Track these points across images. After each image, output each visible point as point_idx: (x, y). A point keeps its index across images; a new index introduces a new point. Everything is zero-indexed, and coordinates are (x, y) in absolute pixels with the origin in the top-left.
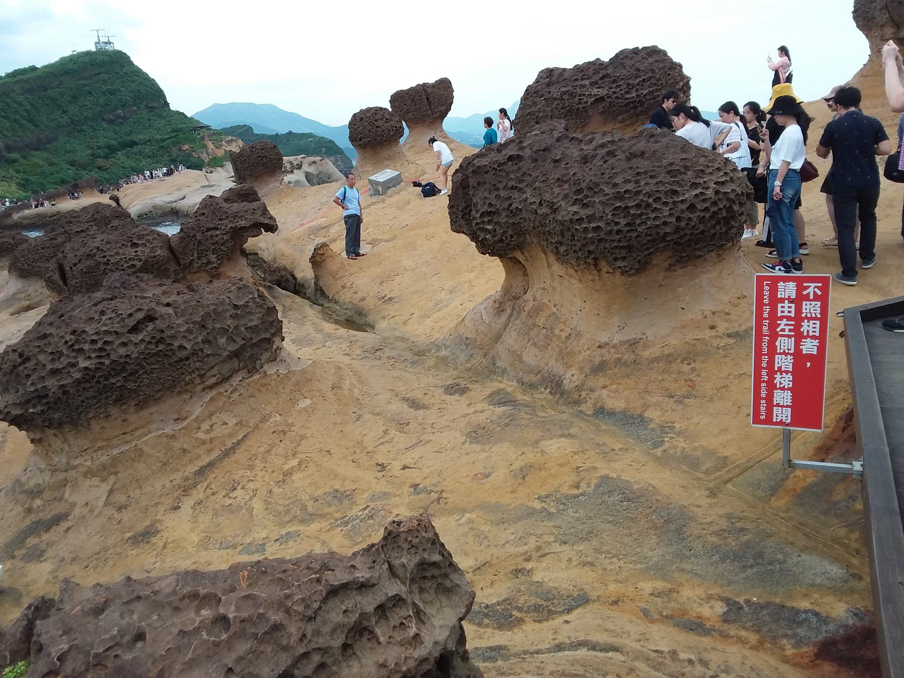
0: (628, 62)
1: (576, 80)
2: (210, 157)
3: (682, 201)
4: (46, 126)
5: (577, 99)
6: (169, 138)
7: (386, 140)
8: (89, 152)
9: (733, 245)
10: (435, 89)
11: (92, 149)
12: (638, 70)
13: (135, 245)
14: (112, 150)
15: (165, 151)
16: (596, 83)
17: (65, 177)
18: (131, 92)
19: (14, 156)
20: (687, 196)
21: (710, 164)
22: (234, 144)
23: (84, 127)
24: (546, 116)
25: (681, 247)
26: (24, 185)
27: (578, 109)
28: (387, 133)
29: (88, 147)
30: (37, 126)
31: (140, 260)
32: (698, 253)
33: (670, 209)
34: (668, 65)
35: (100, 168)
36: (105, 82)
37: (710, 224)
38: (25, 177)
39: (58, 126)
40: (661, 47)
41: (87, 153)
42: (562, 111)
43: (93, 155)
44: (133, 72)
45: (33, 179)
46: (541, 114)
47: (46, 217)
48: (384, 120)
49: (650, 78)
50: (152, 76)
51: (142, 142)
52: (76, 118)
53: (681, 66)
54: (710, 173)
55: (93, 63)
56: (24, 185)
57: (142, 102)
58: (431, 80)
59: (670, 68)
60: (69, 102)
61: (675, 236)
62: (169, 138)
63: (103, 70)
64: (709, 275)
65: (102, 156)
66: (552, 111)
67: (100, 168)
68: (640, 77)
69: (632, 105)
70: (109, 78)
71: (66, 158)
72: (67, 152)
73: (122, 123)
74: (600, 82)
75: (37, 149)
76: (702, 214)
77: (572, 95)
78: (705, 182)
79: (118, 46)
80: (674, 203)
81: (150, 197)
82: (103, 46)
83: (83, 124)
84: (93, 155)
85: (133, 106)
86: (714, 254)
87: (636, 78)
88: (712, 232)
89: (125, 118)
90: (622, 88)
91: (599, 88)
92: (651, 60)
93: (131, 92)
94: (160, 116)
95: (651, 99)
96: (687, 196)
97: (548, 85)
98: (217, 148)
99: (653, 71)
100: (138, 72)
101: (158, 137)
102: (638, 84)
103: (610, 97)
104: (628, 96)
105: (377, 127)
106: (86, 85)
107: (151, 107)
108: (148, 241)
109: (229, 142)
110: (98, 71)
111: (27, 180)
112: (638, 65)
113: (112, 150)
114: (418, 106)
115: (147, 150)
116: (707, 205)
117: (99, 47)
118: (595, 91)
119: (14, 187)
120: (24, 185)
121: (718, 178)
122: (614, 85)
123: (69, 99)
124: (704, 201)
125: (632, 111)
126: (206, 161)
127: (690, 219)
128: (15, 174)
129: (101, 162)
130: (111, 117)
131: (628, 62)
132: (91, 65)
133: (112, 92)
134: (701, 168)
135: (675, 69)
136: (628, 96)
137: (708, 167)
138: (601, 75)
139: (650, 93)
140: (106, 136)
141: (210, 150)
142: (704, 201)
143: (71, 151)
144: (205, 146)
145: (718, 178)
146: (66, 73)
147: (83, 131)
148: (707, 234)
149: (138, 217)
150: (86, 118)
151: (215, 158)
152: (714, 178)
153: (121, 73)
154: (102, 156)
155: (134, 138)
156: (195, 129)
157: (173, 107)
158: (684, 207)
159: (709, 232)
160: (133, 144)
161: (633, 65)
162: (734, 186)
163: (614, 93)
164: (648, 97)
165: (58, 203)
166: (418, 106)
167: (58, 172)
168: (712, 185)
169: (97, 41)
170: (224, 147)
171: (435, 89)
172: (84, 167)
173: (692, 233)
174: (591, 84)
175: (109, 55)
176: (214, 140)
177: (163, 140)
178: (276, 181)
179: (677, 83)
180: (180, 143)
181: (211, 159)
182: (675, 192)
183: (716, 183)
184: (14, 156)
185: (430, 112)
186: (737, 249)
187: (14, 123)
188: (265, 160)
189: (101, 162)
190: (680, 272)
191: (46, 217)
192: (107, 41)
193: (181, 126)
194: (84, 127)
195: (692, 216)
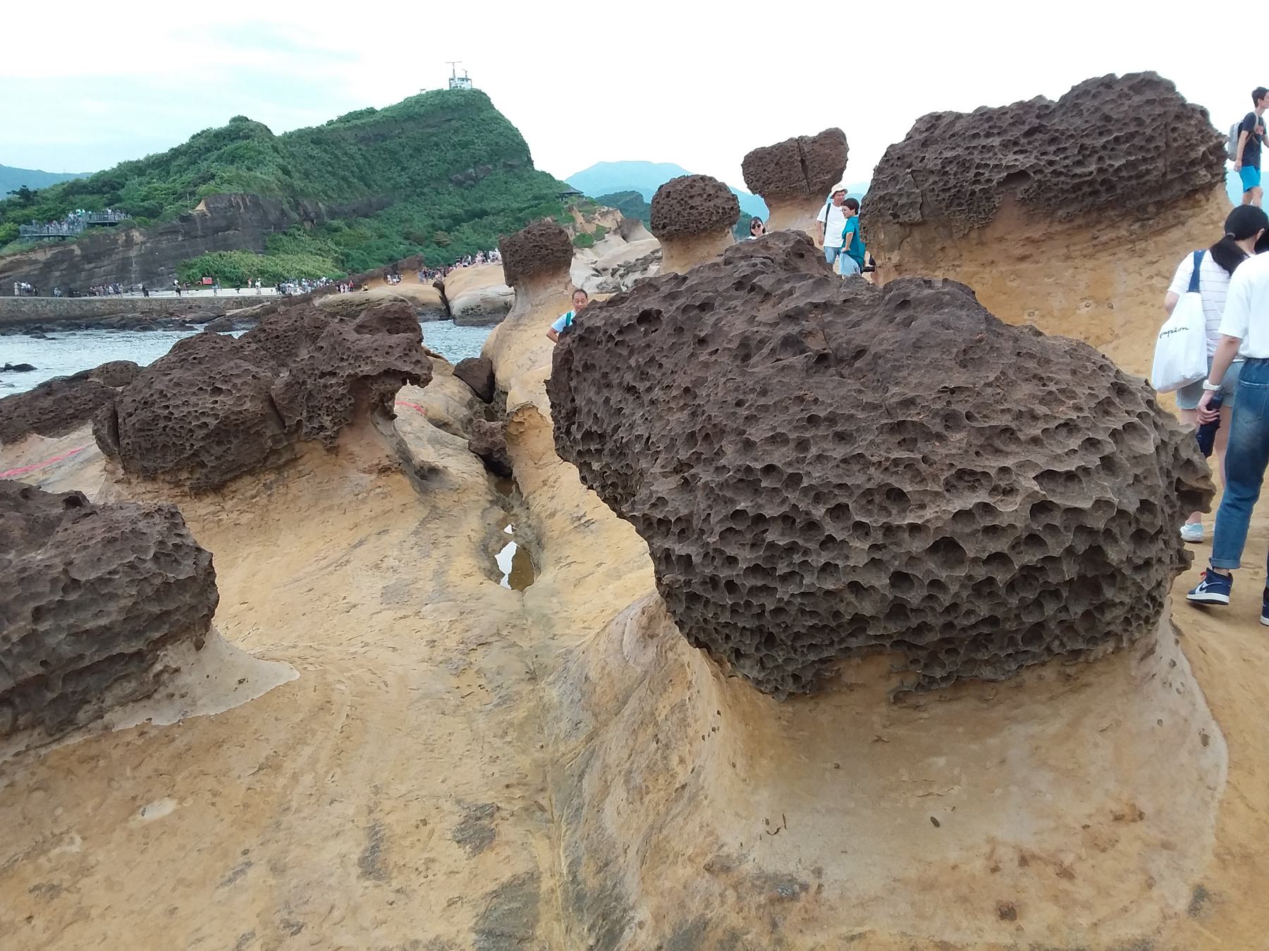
0: (1088, 103)
1: (976, 136)
3: (914, 529)
4: (380, 187)
5: (971, 174)
6: (529, 208)
7: (705, 229)
8: (428, 222)
9: (1118, 649)
10: (816, 146)
12: (1108, 119)
13: (217, 391)
14: (457, 220)
15: (522, 224)
16: (1016, 143)
17: (395, 254)
18: (488, 145)
19: (336, 223)
20: (929, 514)
21: (1041, 410)
22: (610, 217)
23: (425, 190)
24: (912, 204)
25: (923, 654)
26: (342, 262)
27: (973, 193)
28: (707, 218)
29: (428, 215)
30: (369, 186)
31: (216, 416)
32: (987, 673)
33: (874, 547)
34: (1174, 110)
35: (438, 244)
36: (456, 131)
37: (1014, 601)
38: (346, 251)
39: (396, 187)
40: (1164, 74)
41: (426, 223)
42: (942, 196)
43: (433, 226)
44: (491, 119)
45: (354, 253)
46: (904, 200)
47: (352, 305)
48: (705, 196)
49: (1132, 136)
50: (515, 124)
51: (493, 211)
52: (419, 178)
53: (1204, 113)
54: (1035, 441)
56: (343, 261)
57: (499, 159)
58: (812, 130)
59: (1178, 117)
60: (411, 156)
61: (893, 628)
62: (529, 208)
63: (456, 115)
64: (1035, 729)
65: (444, 228)
66: (923, 195)
67: (438, 244)
68: (1109, 132)
69: (1086, 189)
70: (462, 126)
71: (400, 229)
72: (401, 221)
73: (472, 186)
74: (1023, 141)
75: (366, 216)
76: (981, 573)
77: (964, 165)
78: (1004, 470)
79: (477, 84)
80: (888, 529)
81: (481, 286)
82: (459, 83)
83: (426, 186)
84: (433, 226)
85: (489, 163)
86: (1049, 673)
87: (1101, 134)
88: (1030, 619)
89: (476, 180)
90: (1068, 153)
91: (1022, 152)
92: (1137, 99)
93: (488, 145)
94: (520, 178)
95: (1130, 178)
96: (929, 514)
97: (925, 144)
98: (588, 222)
99: (1139, 121)
100: (499, 119)
101: (515, 205)
102: (1104, 147)
103: (1041, 171)
104: (1078, 171)
105: (692, 208)
106: (432, 135)
107: (510, 165)
108: (235, 385)
109: (604, 215)
111: (347, 256)
112: (1106, 109)
113: (457, 220)
114: (785, 173)
115: (500, 222)
116: (1001, 545)
117: (453, 85)
118: (1010, 159)
119: (329, 263)
120: (343, 261)
121: (1057, 458)
122: (1052, 148)
123: (411, 152)
124: (992, 531)
125: (1088, 201)
127: (936, 584)
128: (334, 247)
129: (441, 235)
131: (1088, 103)
132: (442, 108)
133: (464, 145)
134: (1005, 421)
135: (1190, 118)
136: (1078, 171)
137: (1034, 417)
138: (1027, 127)
139: (1131, 165)
140: (452, 202)
141: (578, 225)
142: (992, 531)
143: (407, 220)
144: (573, 219)
145: (1057, 458)
147: (423, 194)
148: (1010, 626)
149: (463, 312)
150: (431, 177)
151: (583, 236)
152: (1041, 460)
153: (478, 119)
154: (444, 228)
155: (487, 205)
156: (562, 196)
157: (538, 166)
158: (918, 545)
159: (1017, 616)
160: (482, 214)
161: (1097, 109)
162: (1106, 488)
163: (1051, 163)
164: (1124, 174)
165: (370, 288)
166: (785, 173)
167: (386, 247)
168: (1028, 483)
169: (452, 77)
170: (597, 222)
171: (816, 146)
172: (419, 241)
173: (949, 626)
174: (1005, 145)
175: (464, 96)
176: (586, 211)
177: (520, 210)
178: (559, 283)
179: (1193, 147)
180: (540, 214)
181: (578, 237)
182: (897, 496)
183: (1047, 476)
184: (336, 223)
185: (804, 183)
186: (1138, 655)
187: (342, 183)
188: (544, 252)
189: (441, 235)
190: (939, 710)
191: (352, 305)
193: (545, 192)
194: (425, 190)
195: (943, 575)
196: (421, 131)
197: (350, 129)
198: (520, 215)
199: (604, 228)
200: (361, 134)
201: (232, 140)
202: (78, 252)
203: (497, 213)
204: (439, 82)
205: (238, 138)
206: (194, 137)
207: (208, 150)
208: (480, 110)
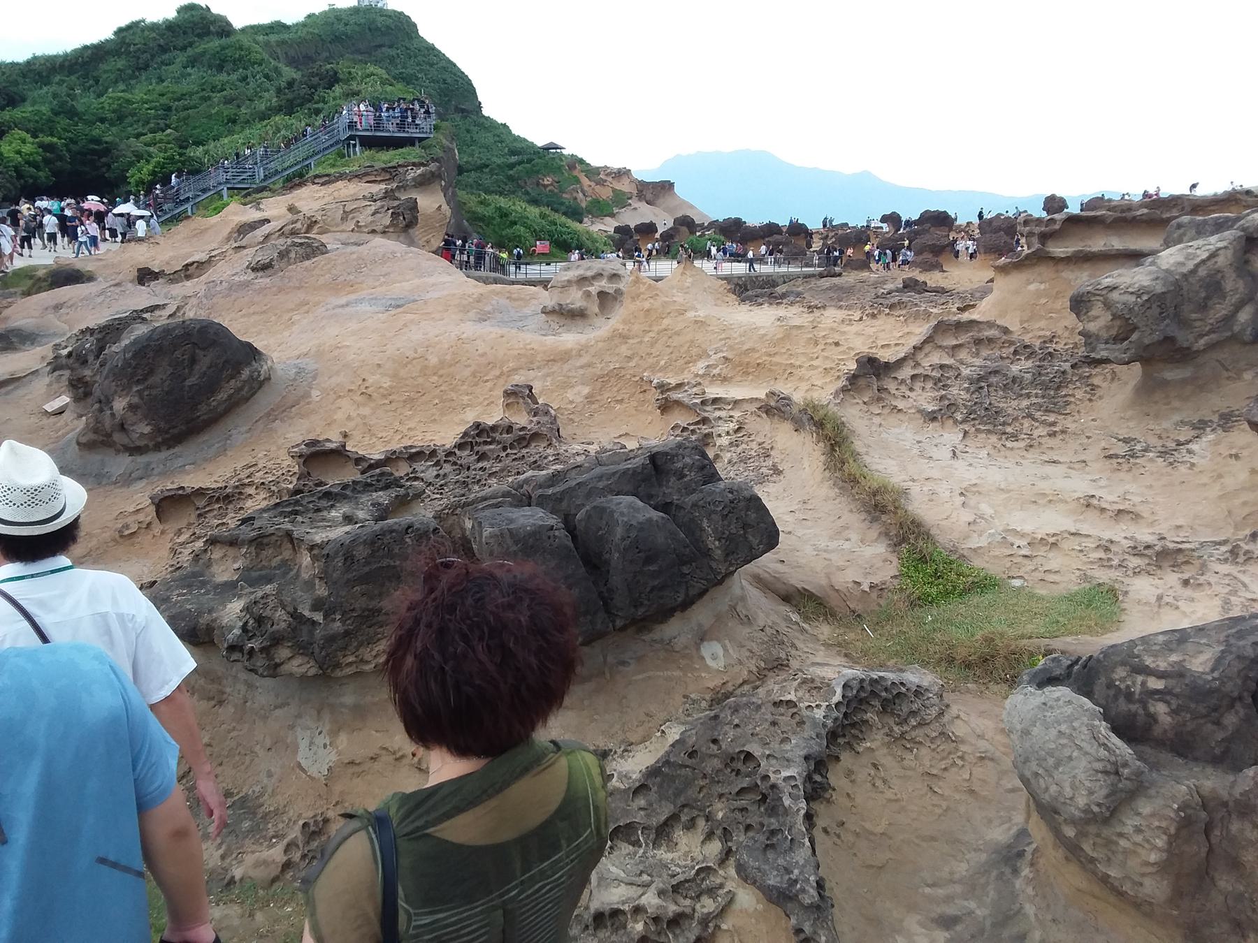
55: (373, 26)
100: (431, 49)
107: (463, 111)
110: (379, 41)
115: (487, 180)
126: (584, 205)
144: (578, 181)
146: (337, 39)
177: (512, 166)
180: (538, 172)
181: (591, 202)
198: (511, 172)
199: (624, 193)
200: (292, 53)
201: (200, 36)
203: (480, 168)
205: (208, 33)
206: (120, 31)
207: (163, 49)
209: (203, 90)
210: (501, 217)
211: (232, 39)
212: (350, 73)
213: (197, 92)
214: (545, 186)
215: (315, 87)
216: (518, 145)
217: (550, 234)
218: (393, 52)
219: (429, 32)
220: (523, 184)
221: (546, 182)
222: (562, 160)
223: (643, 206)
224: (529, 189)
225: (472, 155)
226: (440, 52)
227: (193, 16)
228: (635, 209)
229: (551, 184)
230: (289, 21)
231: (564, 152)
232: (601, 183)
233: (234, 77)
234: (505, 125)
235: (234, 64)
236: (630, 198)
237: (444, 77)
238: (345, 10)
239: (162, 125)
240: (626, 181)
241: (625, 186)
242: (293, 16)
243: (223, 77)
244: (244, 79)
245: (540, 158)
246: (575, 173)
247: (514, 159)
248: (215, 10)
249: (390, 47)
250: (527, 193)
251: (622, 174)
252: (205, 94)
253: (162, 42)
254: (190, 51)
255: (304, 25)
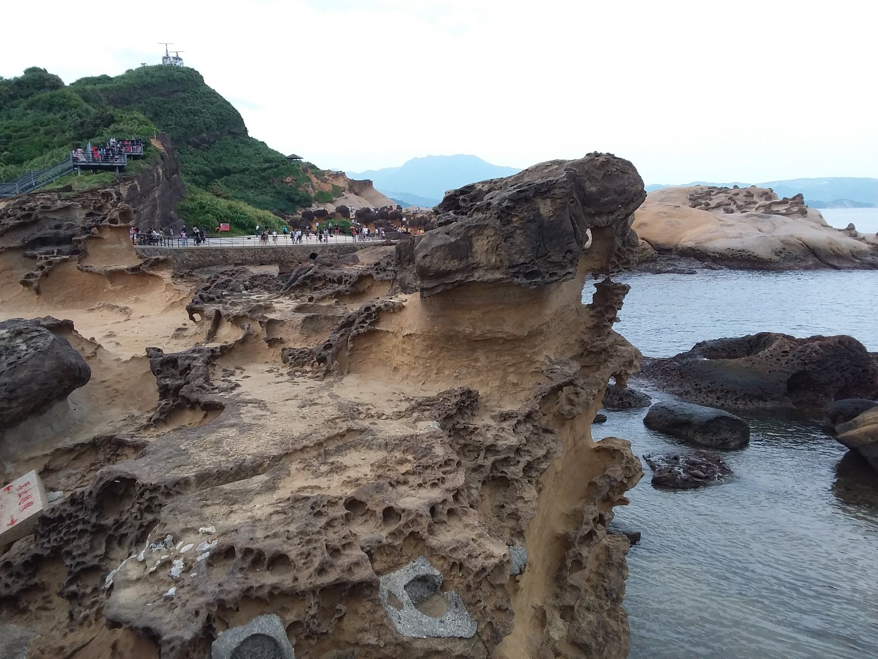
2: (317, 191)
11: (188, 174)
36: (184, 100)
55: (171, 79)
79: (188, 62)
85: (217, 130)
100: (213, 93)
107: (234, 133)
115: (247, 179)
117: (168, 62)
126: (313, 195)
130: (196, 140)
141: (314, 184)
144: (309, 180)
146: (146, 87)
160: (228, 172)
177: (264, 170)
180: (282, 174)
192: (175, 55)
196: (155, 98)
197: (102, 90)
198: (264, 174)
199: (340, 188)
200: (111, 96)
201: (39, 89)
202: (139, 189)
203: (243, 171)
204: (155, 60)
207: (13, 97)
208: (198, 86)
209: (35, 125)
210: (201, 208)
211: (59, 91)
212: (121, 117)
213: (31, 126)
214: (287, 183)
215: (97, 126)
216: (271, 156)
217: (232, 219)
218: (184, 95)
219: (212, 81)
220: (271, 182)
221: (287, 181)
222: (299, 166)
223: (352, 196)
224: (276, 185)
225: (237, 162)
226: (219, 95)
227: (34, 76)
228: (347, 198)
229: (291, 182)
230: (112, 74)
231: (303, 160)
232: (325, 181)
233: (58, 116)
234: (263, 143)
235: (59, 107)
236: (344, 191)
237: (221, 111)
238: (151, 67)
239: (3, 149)
240: (341, 179)
241: (340, 183)
242: (115, 70)
243: (51, 116)
244: (64, 117)
245: (283, 165)
246: (308, 175)
247: (267, 165)
248: (50, 72)
249: (184, 91)
250: (274, 187)
251: (339, 175)
252: (36, 127)
253: (12, 93)
254: (30, 99)
255: (122, 77)
